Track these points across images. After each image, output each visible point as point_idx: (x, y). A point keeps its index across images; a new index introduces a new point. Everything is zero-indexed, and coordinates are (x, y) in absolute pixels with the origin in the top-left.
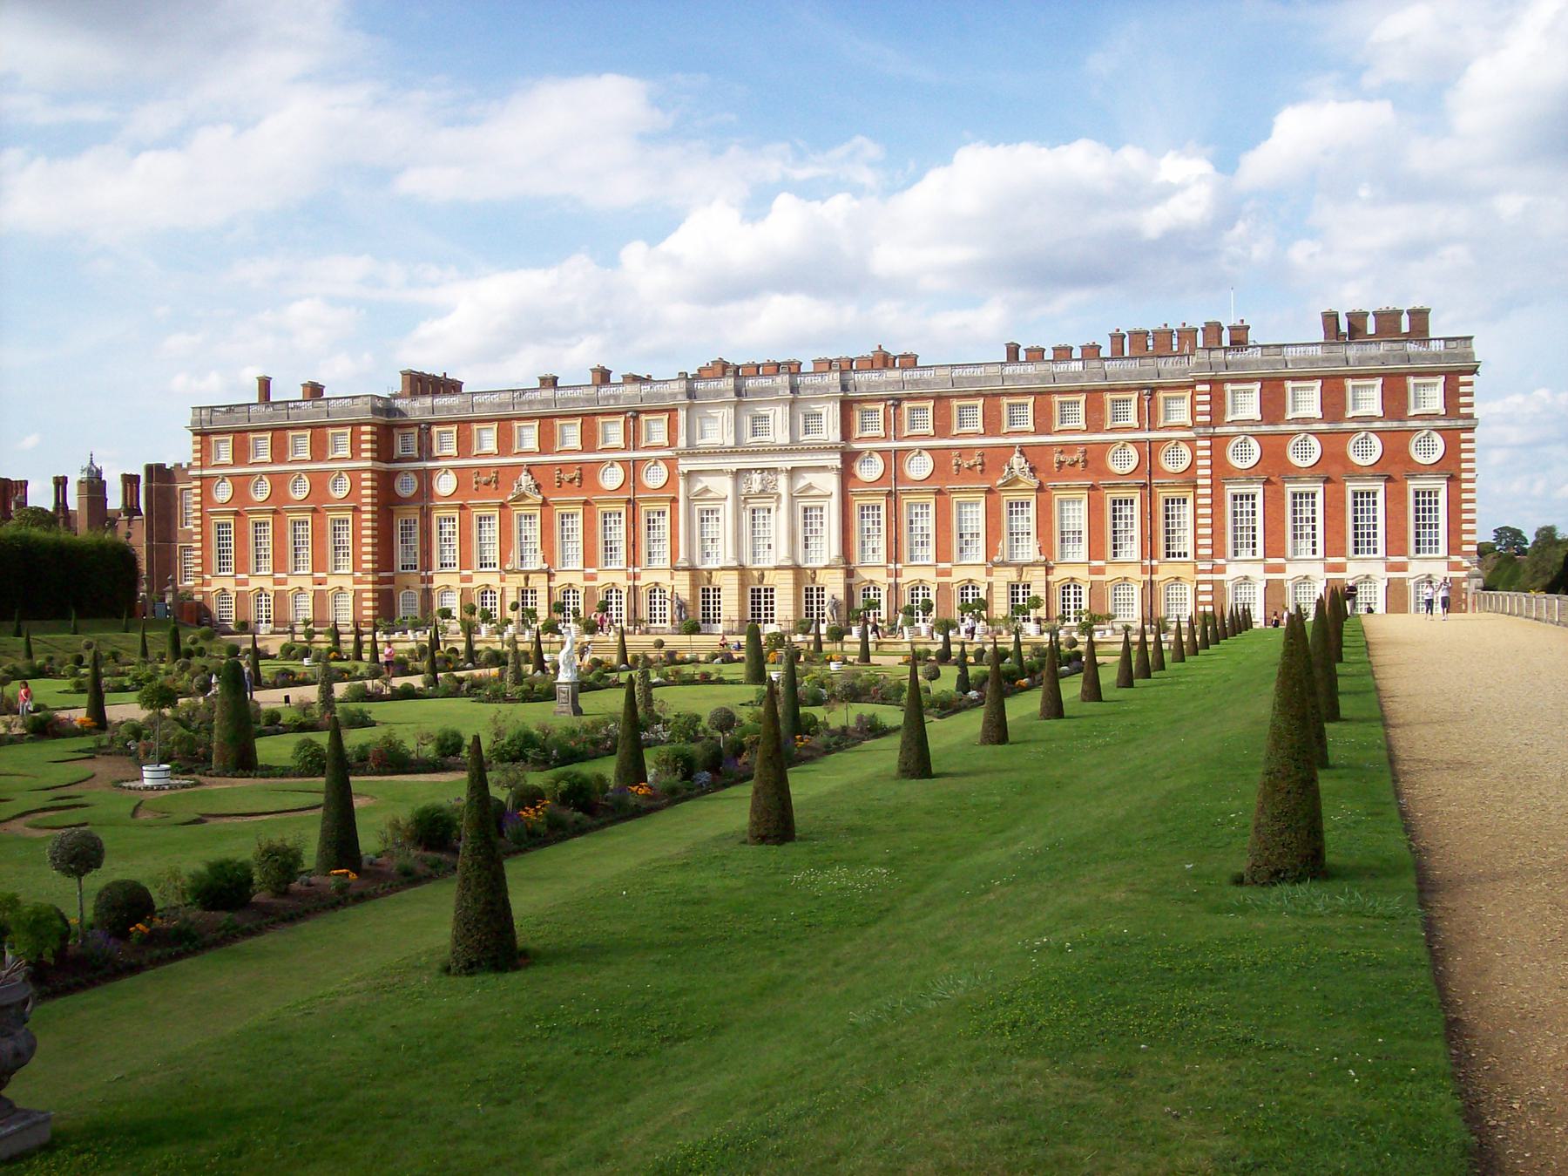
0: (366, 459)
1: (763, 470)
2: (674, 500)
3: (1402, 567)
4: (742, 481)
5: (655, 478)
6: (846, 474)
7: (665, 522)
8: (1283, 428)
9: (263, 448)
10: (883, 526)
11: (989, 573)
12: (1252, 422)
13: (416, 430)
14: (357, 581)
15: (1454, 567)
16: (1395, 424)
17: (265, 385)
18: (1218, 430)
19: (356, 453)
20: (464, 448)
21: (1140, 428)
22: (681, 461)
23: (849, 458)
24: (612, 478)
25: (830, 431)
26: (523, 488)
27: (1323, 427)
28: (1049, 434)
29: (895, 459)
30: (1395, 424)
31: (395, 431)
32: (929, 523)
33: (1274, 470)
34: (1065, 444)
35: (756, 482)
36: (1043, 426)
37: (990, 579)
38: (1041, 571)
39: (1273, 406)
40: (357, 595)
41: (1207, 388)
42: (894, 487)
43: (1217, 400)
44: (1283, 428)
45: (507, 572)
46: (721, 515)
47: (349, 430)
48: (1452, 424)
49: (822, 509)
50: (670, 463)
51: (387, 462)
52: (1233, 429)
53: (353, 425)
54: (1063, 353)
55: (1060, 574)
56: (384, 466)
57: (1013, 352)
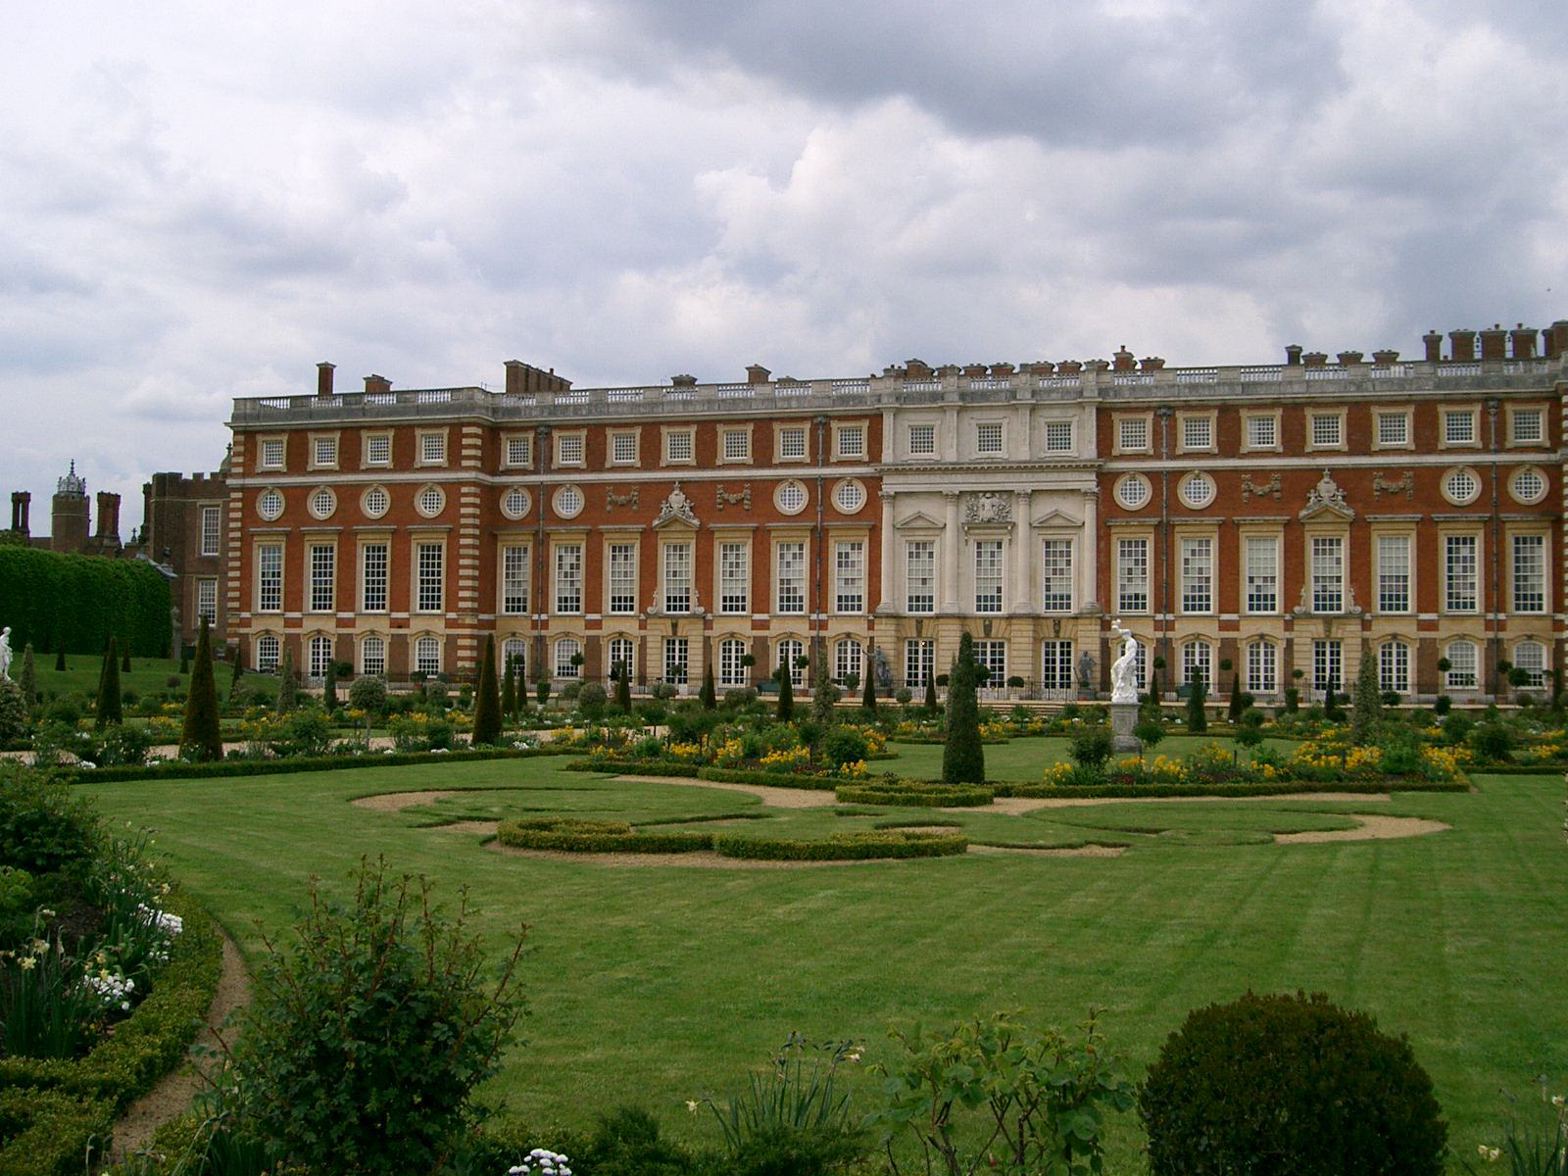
1: (993, 493)
2: (875, 532)
4: (963, 507)
5: (849, 501)
7: (862, 558)
10: (1149, 565)
11: (1289, 626)
13: (531, 435)
14: (450, 624)
17: (326, 373)
19: (455, 460)
20: (596, 459)
21: (1486, 450)
22: (886, 479)
23: (1106, 480)
24: (791, 502)
25: (1083, 444)
26: (1326, 501)
28: (1368, 453)
29: (1165, 483)
31: (503, 436)
32: (1211, 564)
36: (1360, 442)
37: (1292, 635)
38: (1354, 627)
40: (451, 643)
42: (1165, 517)
45: (648, 616)
46: (936, 550)
47: (446, 431)
49: (1068, 544)
50: (873, 483)
51: (494, 473)
55: (1380, 629)
56: (489, 479)
57: (1294, 354)
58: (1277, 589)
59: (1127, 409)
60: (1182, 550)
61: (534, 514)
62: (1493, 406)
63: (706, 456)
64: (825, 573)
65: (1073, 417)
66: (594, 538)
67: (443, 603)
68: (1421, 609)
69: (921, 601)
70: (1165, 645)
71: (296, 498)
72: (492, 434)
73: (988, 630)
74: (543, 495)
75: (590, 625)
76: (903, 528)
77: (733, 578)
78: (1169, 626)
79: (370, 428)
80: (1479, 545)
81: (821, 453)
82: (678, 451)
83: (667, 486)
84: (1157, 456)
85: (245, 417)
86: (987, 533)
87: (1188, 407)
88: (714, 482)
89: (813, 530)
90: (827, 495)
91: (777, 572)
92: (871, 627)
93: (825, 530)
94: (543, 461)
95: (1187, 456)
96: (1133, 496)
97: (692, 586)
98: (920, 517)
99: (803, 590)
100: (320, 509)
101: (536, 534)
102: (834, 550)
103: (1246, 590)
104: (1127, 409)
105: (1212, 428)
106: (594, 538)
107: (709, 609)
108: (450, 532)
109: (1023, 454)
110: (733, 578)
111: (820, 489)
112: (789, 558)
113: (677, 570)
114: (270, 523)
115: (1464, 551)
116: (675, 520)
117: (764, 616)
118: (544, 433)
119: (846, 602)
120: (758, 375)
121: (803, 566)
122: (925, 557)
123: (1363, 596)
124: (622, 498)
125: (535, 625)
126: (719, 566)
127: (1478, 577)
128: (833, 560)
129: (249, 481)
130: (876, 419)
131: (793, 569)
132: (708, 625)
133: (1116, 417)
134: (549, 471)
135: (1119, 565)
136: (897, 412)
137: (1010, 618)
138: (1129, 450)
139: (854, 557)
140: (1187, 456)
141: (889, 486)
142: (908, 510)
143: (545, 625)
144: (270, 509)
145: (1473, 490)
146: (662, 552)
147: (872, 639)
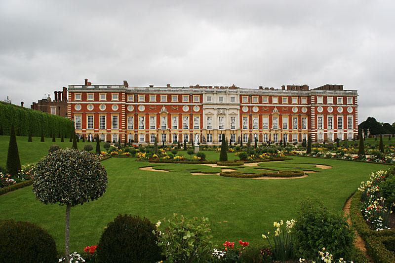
0: (123, 101)
3: (346, 131)
7: (199, 120)
8: (327, 105)
9: (90, 98)
15: (354, 131)
19: (120, 100)
20: (147, 100)
21: (298, 104)
23: (241, 107)
24: (186, 109)
25: (237, 101)
27: (334, 105)
29: (250, 108)
30: (345, 106)
32: (258, 121)
33: (325, 113)
36: (280, 102)
38: (280, 131)
39: (325, 101)
40: (120, 135)
42: (251, 113)
44: (327, 105)
48: (354, 106)
50: (201, 107)
53: (119, 93)
54: (267, 89)
55: (284, 132)
58: (268, 125)
59: (244, 95)
60: (253, 119)
61: (134, 111)
63: (169, 100)
64: (192, 122)
65: (235, 96)
66: (147, 116)
67: (118, 127)
68: (309, 129)
70: (251, 134)
71: (84, 106)
72: (126, 94)
73: (221, 132)
74: (136, 107)
75: (146, 132)
77: (175, 122)
79: (101, 93)
80: (297, 119)
81: (191, 101)
82: (163, 99)
83: (162, 106)
84: (249, 103)
85: (71, 89)
86: (221, 115)
87: (254, 95)
88: (171, 105)
89: (190, 115)
90: (192, 108)
92: (201, 131)
93: (192, 114)
94: (136, 100)
95: (254, 103)
96: (245, 110)
97: (167, 124)
99: (188, 125)
100: (90, 108)
101: (135, 114)
102: (194, 118)
103: (263, 125)
104: (244, 95)
105: (258, 99)
106: (147, 116)
107: (171, 129)
108: (119, 114)
109: (228, 102)
110: (175, 122)
111: (191, 107)
113: (164, 121)
114: (78, 111)
116: (164, 112)
118: (136, 95)
120: (261, 88)
121: (188, 120)
122: (210, 119)
123: (281, 127)
124: (153, 108)
125: (135, 132)
126: (172, 121)
127: (297, 124)
128: (194, 120)
129: (73, 102)
130: (201, 95)
131: (186, 121)
132: (170, 132)
133: (242, 97)
134: (137, 102)
135: (243, 121)
137: (226, 130)
140: (254, 103)
142: (207, 111)
143: (137, 132)
144: (78, 108)
145: (296, 110)
146: (161, 118)
147: (201, 134)
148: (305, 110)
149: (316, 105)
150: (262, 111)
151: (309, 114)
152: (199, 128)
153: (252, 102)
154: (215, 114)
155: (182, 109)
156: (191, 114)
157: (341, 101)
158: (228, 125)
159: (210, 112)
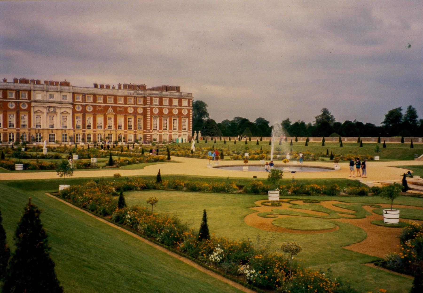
6: (74, 109)
7: (27, 118)
12: (157, 105)
16: (180, 107)
18: (152, 106)
21: (134, 105)
23: (74, 105)
24: (12, 106)
25: (69, 98)
27: (169, 107)
30: (180, 107)
33: (161, 114)
34: (119, 106)
35: (52, 110)
36: (115, 102)
39: (161, 103)
41: (150, 98)
43: (151, 100)
44: (162, 107)
52: (154, 106)
58: (102, 125)
60: (87, 118)
62: (135, 98)
69: (38, 126)
73: (52, 131)
76: (35, 112)
78: (85, 131)
87: (88, 94)
90: (19, 105)
91: (9, 120)
92: (29, 130)
95: (88, 102)
98: (39, 110)
99: (14, 123)
103: (97, 125)
109: (59, 100)
112: (11, 117)
115: (131, 120)
117: (6, 128)
119: (23, 126)
122: (39, 118)
123: (116, 127)
128: (21, 118)
131: (13, 119)
133: (75, 95)
135: (76, 120)
136: (34, 90)
138: (78, 101)
139: (25, 117)
140: (88, 102)
141: (33, 104)
142: (36, 109)
147: (30, 133)
148: (140, 111)
149: (152, 106)
150: (95, 112)
151: (144, 115)
152: (27, 126)
153: (85, 100)
154: (45, 114)
155: (7, 105)
156: (18, 111)
157: (175, 102)
158: (59, 124)
159: (39, 110)
